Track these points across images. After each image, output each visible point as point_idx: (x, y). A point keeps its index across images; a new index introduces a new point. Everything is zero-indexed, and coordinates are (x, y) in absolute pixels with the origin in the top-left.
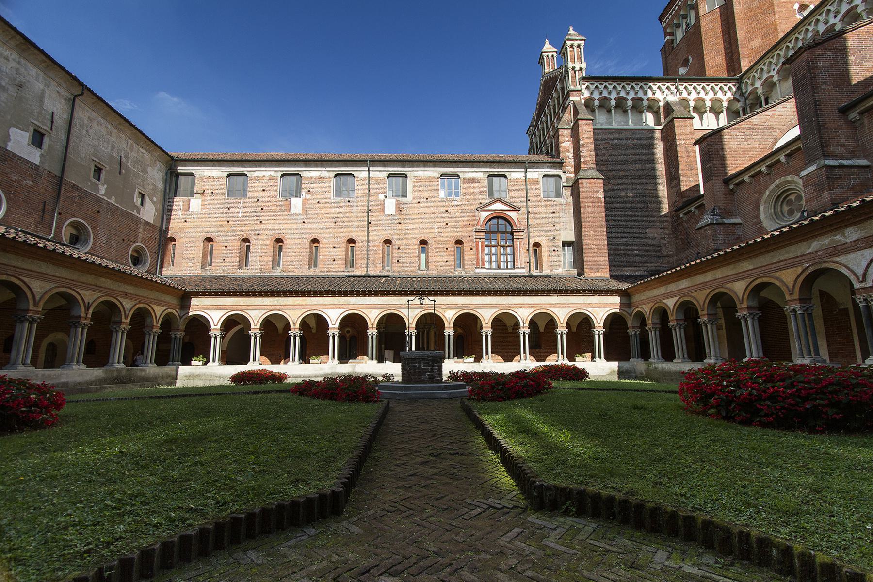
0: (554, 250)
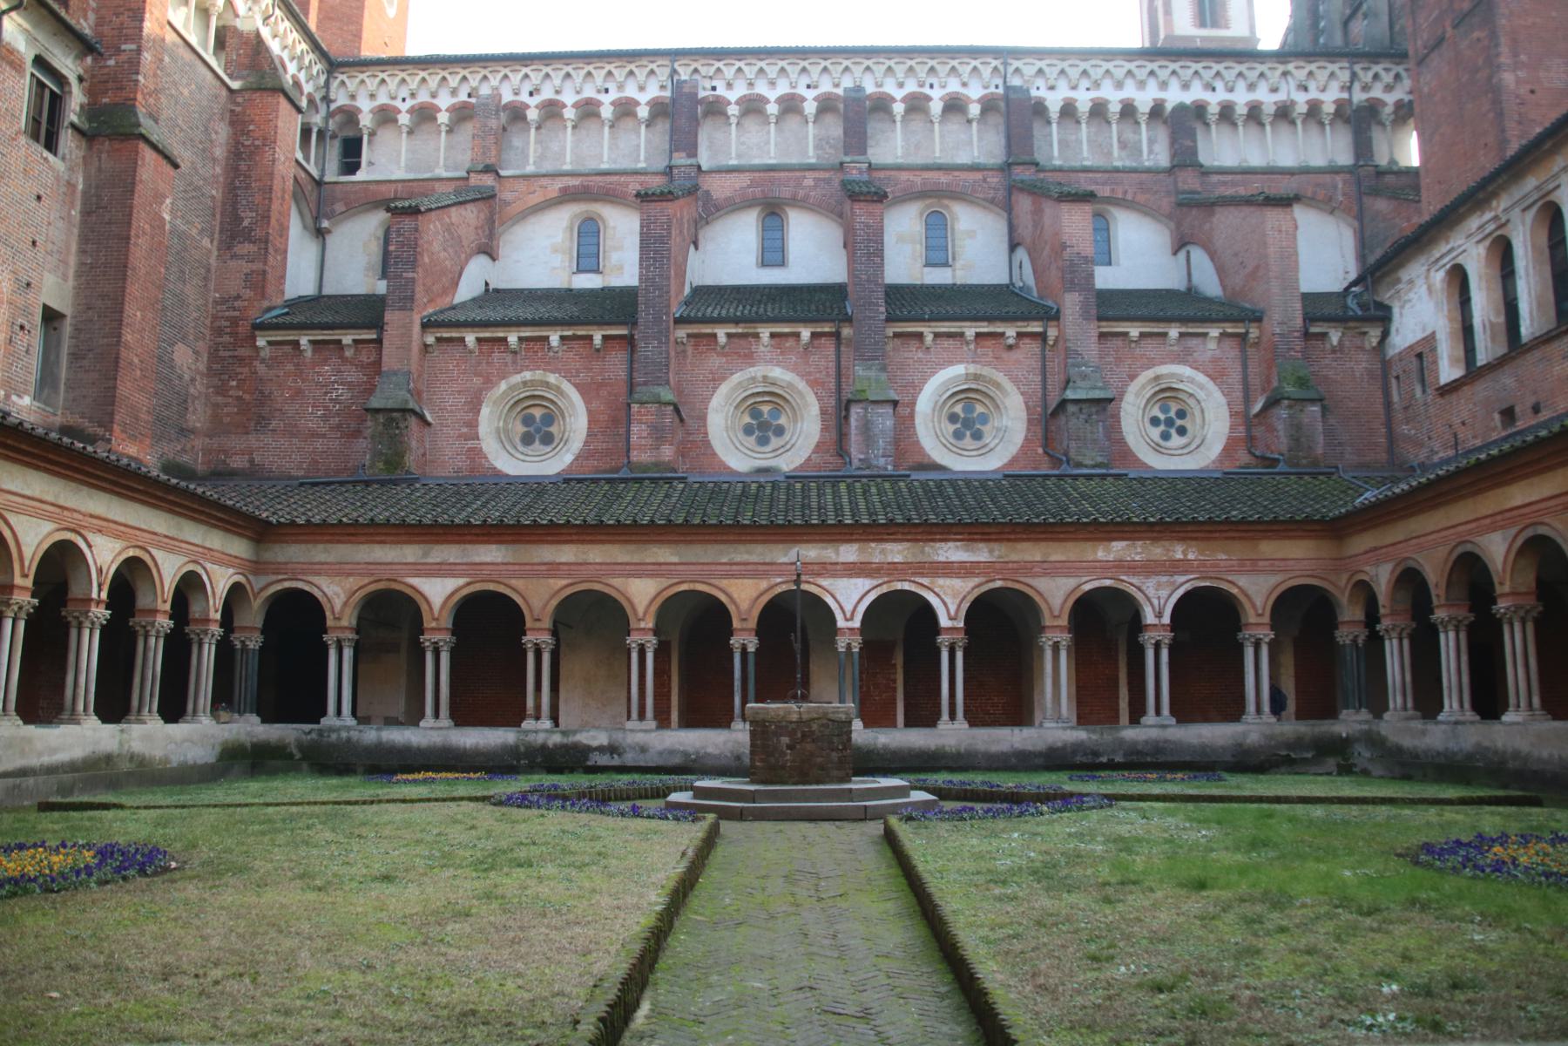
0: (22, 327)
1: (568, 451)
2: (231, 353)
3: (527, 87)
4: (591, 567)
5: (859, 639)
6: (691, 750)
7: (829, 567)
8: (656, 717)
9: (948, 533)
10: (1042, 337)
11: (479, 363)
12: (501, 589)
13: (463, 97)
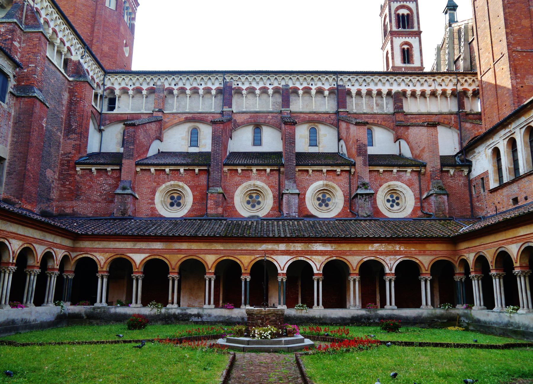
1: (186, 209)
2: (67, 173)
3: (173, 83)
4: (193, 251)
5: (286, 277)
6: (226, 315)
7: (275, 252)
8: (214, 304)
9: (317, 240)
10: (349, 171)
11: (155, 178)
12: (161, 258)
13: (151, 85)
